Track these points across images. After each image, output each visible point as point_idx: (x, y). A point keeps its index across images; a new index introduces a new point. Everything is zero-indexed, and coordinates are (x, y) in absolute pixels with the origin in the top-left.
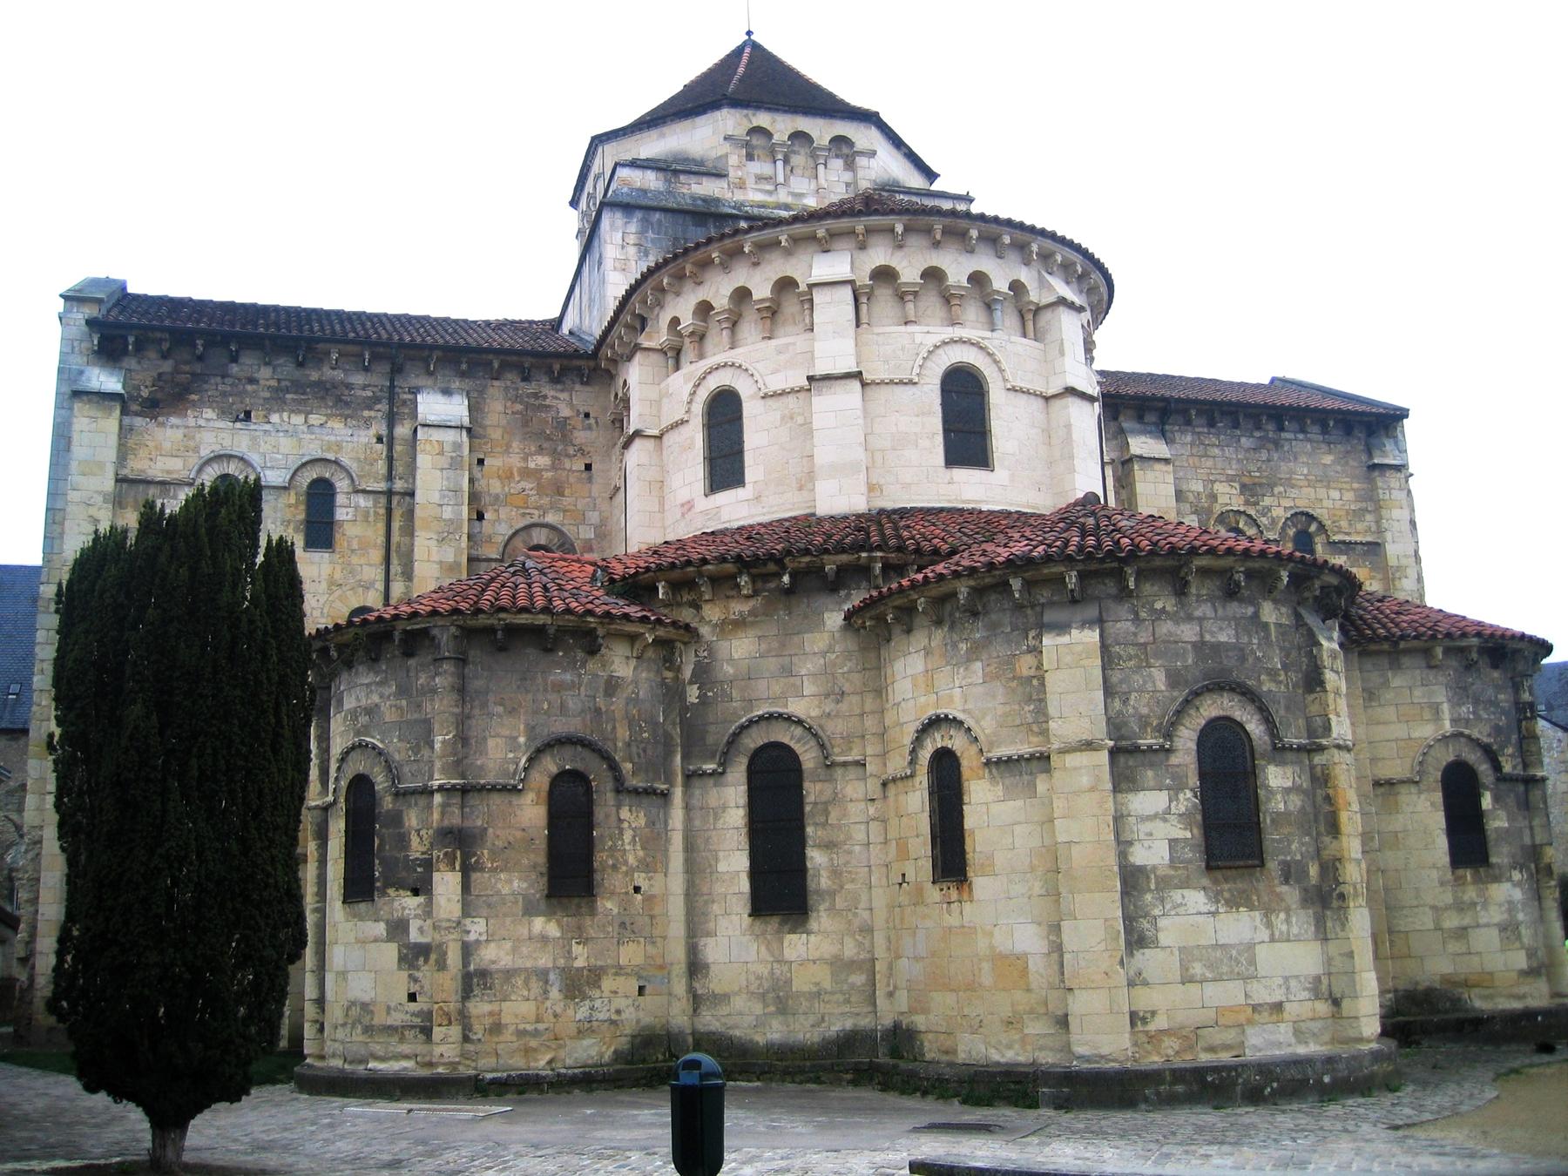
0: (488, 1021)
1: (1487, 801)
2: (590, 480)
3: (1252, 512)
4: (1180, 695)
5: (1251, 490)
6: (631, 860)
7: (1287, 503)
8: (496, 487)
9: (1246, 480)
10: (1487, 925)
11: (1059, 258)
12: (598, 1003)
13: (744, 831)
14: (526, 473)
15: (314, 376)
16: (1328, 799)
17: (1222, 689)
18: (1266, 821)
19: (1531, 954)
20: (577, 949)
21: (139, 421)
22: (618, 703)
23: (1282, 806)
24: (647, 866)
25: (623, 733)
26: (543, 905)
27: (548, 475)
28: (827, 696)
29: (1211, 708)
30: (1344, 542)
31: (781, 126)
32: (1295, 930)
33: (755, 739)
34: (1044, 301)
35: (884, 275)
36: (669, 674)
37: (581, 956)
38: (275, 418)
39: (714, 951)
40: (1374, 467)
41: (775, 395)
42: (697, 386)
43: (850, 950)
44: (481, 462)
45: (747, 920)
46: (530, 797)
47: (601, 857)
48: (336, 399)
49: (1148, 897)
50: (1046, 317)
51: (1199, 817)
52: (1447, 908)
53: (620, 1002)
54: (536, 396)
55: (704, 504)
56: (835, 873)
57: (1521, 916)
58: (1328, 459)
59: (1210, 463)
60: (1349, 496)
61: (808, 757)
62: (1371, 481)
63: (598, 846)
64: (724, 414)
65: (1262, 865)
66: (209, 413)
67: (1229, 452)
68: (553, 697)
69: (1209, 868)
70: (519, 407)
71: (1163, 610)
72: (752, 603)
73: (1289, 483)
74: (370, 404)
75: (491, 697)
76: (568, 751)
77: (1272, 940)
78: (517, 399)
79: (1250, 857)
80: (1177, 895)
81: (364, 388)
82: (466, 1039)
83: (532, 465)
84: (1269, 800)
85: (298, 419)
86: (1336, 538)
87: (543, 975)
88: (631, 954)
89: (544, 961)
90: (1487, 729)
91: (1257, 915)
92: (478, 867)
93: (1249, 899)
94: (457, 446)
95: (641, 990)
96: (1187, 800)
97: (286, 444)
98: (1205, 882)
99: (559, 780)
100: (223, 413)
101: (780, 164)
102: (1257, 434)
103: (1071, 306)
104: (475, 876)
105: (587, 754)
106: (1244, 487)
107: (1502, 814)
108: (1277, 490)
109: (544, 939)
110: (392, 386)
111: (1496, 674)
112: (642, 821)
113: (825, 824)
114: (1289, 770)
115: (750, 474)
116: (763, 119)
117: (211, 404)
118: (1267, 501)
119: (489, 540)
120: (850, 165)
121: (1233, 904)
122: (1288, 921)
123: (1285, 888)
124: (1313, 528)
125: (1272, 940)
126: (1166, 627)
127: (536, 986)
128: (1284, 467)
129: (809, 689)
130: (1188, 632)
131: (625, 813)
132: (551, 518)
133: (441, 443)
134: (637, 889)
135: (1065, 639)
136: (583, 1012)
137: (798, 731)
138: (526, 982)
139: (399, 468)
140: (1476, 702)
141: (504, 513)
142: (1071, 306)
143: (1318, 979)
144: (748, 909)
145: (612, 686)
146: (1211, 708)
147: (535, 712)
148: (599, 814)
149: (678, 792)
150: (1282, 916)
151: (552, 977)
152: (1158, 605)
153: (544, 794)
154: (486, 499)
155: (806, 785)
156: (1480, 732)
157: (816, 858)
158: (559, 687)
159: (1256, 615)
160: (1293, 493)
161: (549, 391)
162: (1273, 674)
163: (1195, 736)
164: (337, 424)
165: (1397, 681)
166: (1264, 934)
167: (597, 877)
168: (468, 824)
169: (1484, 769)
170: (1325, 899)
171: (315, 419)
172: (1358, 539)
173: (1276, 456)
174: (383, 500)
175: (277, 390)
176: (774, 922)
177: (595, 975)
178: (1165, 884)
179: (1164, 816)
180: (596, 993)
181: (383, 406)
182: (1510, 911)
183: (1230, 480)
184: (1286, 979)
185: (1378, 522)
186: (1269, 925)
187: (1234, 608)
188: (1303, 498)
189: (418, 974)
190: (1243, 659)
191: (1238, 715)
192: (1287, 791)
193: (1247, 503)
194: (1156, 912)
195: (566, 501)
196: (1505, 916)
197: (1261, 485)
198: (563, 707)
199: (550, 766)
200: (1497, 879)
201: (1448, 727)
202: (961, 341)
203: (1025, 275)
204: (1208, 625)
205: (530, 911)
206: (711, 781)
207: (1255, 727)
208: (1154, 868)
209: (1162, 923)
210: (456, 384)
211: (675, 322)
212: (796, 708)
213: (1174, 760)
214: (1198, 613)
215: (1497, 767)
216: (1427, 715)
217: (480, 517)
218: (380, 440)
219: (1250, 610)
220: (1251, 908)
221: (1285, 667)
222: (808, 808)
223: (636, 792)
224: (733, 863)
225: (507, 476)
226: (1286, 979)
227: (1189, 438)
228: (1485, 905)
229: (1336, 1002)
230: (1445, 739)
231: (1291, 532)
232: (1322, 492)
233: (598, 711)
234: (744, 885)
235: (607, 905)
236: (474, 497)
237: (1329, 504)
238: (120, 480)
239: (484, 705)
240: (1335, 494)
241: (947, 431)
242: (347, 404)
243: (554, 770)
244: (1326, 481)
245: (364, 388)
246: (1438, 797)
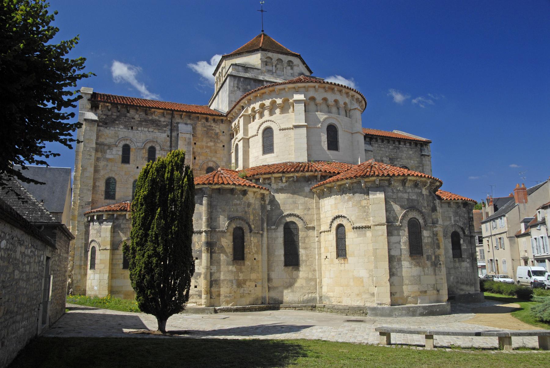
0: (217, 293)
1: (462, 242)
2: (224, 150)
6: (254, 251)
8: (199, 150)
9: (391, 157)
11: (356, 97)
12: (245, 289)
13: (283, 244)
14: (207, 147)
15: (150, 118)
16: (437, 239)
20: (240, 274)
21: (102, 128)
22: (251, 210)
24: (257, 253)
25: (252, 217)
26: (231, 263)
27: (213, 148)
28: (305, 209)
31: (275, 56)
34: (352, 108)
35: (313, 99)
36: (263, 202)
37: (241, 276)
38: (139, 129)
39: (273, 275)
40: (422, 155)
41: (283, 130)
42: (260, 126)
43: (310, 276)
44: (195, 144)
45: (283, 267)
46: (229, 234)
47: (246, 250)
48: (156, 124)
49: (395, 263)
50: (352, 112)
51: (408, 243)
52: (452, 268)
53: (250, 289)
54: (210, 126)
55: (262, 157)
56: (307, 255)
57: (469, 271)
58: (411, 152)
59: (382, 152)
60: (416, 162)
61: (300, 225)
62: (422, 159)
64: (268, 133)
66: (121, 127)
67: (387, 149)
68: (234, 207)
70: (206, 129)
71: (399, 190)
72: (285, 184)
73: (401, 158)
74: (166, 126)
75: (218, 207)
76: (238, 221)
77: (425, 275)
78: (205, 127)
79: (418, 254)
81: (164, 122)
82: (211, 298)
83: (209, 145)
88: (253, 276)
90: (462, 223)
92: (215, 252)
93: (419, 264)
94: (190, 139)
95: (256, 286)
99: (236, 229)
100: (126, 127)
101: (274, 67)
103: (359, 110)
104: (213, 255)
106: (390, 158)
107: (465, 245)
108: (399, 160)
110: (172, 122)
111: (464, 209)
112: (256, 241)
113: (304, 243)
115: (275, 150)
116: (270, 54)
117: (122, 124)
119: (197, 165)
120: (292, 69)
122: (428, 270)
123: (427, 262)
125: (425, 275)
126: (400, 194)
127: (230, 284)
128: (400, 154)
129: (300, 207)
130: (406, 196)
131: (252, 239)
132: (214, 159)
133: (185, 138)
134: (255, 259)
135: (375, 197)
137: (297, 219)
138: (227, 283)
139: (173, 144)
140: (460, 216)
141: (201, 157)
142: (359, 110)
143: (434, 285)
144: (283, 264)
145: (249, 205)
147: (230, 211)
149: (265, 233)
151: (234, 282)
152: (398, 189)
153: (232, 233)
154: (197, 154)
155: (300, 232)
156: (460, 224)
157: (302, 252)
158: (236, 205)
159: (421, 192)
160: (402, 161)
161: (213, 125)
162: (425, 207)
163: (407, 222)
166: (423, 273)
167: (245, 255)
168: (212, 241)
169: (461, 233)
170: (435, 264)
171: (150, 130)
175: (140, 121)
176: (291, 268)
181: (169, 127)
183: (387, 157)
185: (423, 169)
186: (424, 271)
187: (417, 190)
189: (198, 281)
190: (418, 203)
191: (417, 217)
192: (428, 237)
194: (397, 267)
195: (218, 155)
198: (237, 211)
199: (234, 226)
200: (463, 261)
202: (332, 118)
203: (347, 100)
204: (410, 194)
206: (273, 231)
207: (421, 221)
208: (397, 256)
209: (398, 270)
211: (254, 108)
212: (296, 212)
214: (408, 191)
215: (464, 233)
216: (448, 219)
217: (195, 158)
218: (168, 136)
219: (420, 191)
220: (420, 266)
221: (428, 205)
222: (300, 238)
224: (280, 252)
225: (202, 148)
227: (377, 145)
228: (461, 268)
229: (438, 291)
230: (452, 226)
232: (409, 161)
233: (246, 212)
234: (283, 258)
235: (248, 263)
236: (194, 153)
238: (97, 144)
239: (216, 209)
240: (412, 162)
242: (159, 126)
243: (235, 227)
244: (410, 158)
245: (164, 122)
246: (450, 240)
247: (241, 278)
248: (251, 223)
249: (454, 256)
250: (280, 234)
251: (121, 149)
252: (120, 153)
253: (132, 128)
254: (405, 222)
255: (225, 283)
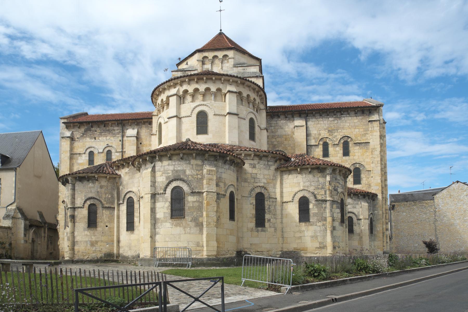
1: (311, 206)
3: (330, 137)
4: (167, 182)
5: (330, 131)
6: (105, 220)
7: (341, 134)
9: (330, 129)
10: (308, 236)
17: (178, 180)
18: (186, 208)
19: (320, 243)
20: (93, 237)
23: (192, 205)
25: (104, 196)
29: (174, 184)
30: (358, 143)
32: (192, 232)
33: (128, 196)
37: (94, 239)
38: (100, 138)
46: (85, 209)
47: (98, 220)
51: (170, 208)
57: (318, 234)
58: (356, 121)
59: (319, 125)
60: (362, 130)
63: (98, 217)
65: (184, 218)
69: (171, 218)
73: (343, 128)
74: (118, 134)
76: (92, 200)
77: (185, 234)
79: (182, 216)
80: (164, 224)
84: (188, 204)
85: (105, 138)
86: (356, 142)
87: (86, 242)
89: (87, 239)
91: (182, 228)
93: (180, 225)
94: (134, 141)
96: (168, 204)
97: (102, 143)
98: (170, 221)
99: (90, 206)
100: (91, 138)
102: (334, 116)
105: (96, 200)
106: (329, 131)
107: (316, 209)
108: (339, 131)
109: (87, 235)
114: (195, 197)
118: (336, 134)
121: (176, 226)
124: (349, 140)
129: (136, 185)
134: (107, 226)
136: (94, 249)
146: (174, 184)
148: (98, 212)
150: (189, 228)
156: (311, 189)
160: (344, 131)
164: (112, 138)
165: (290, 176)
166: (184, 232)
167: (98, 224)
169: (311, 199)
170: (200, 225)
171: (108, 138)
172: (363, 142)
173: (339, 121)
174: (121, 153)
177: (97, 242)
178: (162, 222)
179: (163, 208)
180: (97, 245)
181: (121, 134)
182: (315, 233)
183: (325, 130)
184: (188, 242)
186: (185, 230)
188: (346, 132)
191: (181, 185)
193: (330, 135)
196: (313, 234)
197: (334, 130)
199: (88, 203)
200: (311, 225)
201: (302, 188)
205: (84, 230)
207: (185, 188)
210: (136, 127)
213: (166, 195)
215: (315, 197)
218: (120, 141)
220: (180, 227)
223: (106, 207)
226: (188, 242)
231: (342, 141)
232: (353, 130)
233: (98, 192)
235: (99, 229)
237: (355, 133)
240: (357, 130)
241: (197, 127)
243: (89, 204)
244: (355, 127)
245: (117, 130)
246: (297, 205)
247: (94, 240)
248: (103, 201)
249: (301, 220)
250: (124, 208)
251: (88, 155)
252: (87, 158)
253: (95, 138)
254: (169, 191)
255: (82, 243)
